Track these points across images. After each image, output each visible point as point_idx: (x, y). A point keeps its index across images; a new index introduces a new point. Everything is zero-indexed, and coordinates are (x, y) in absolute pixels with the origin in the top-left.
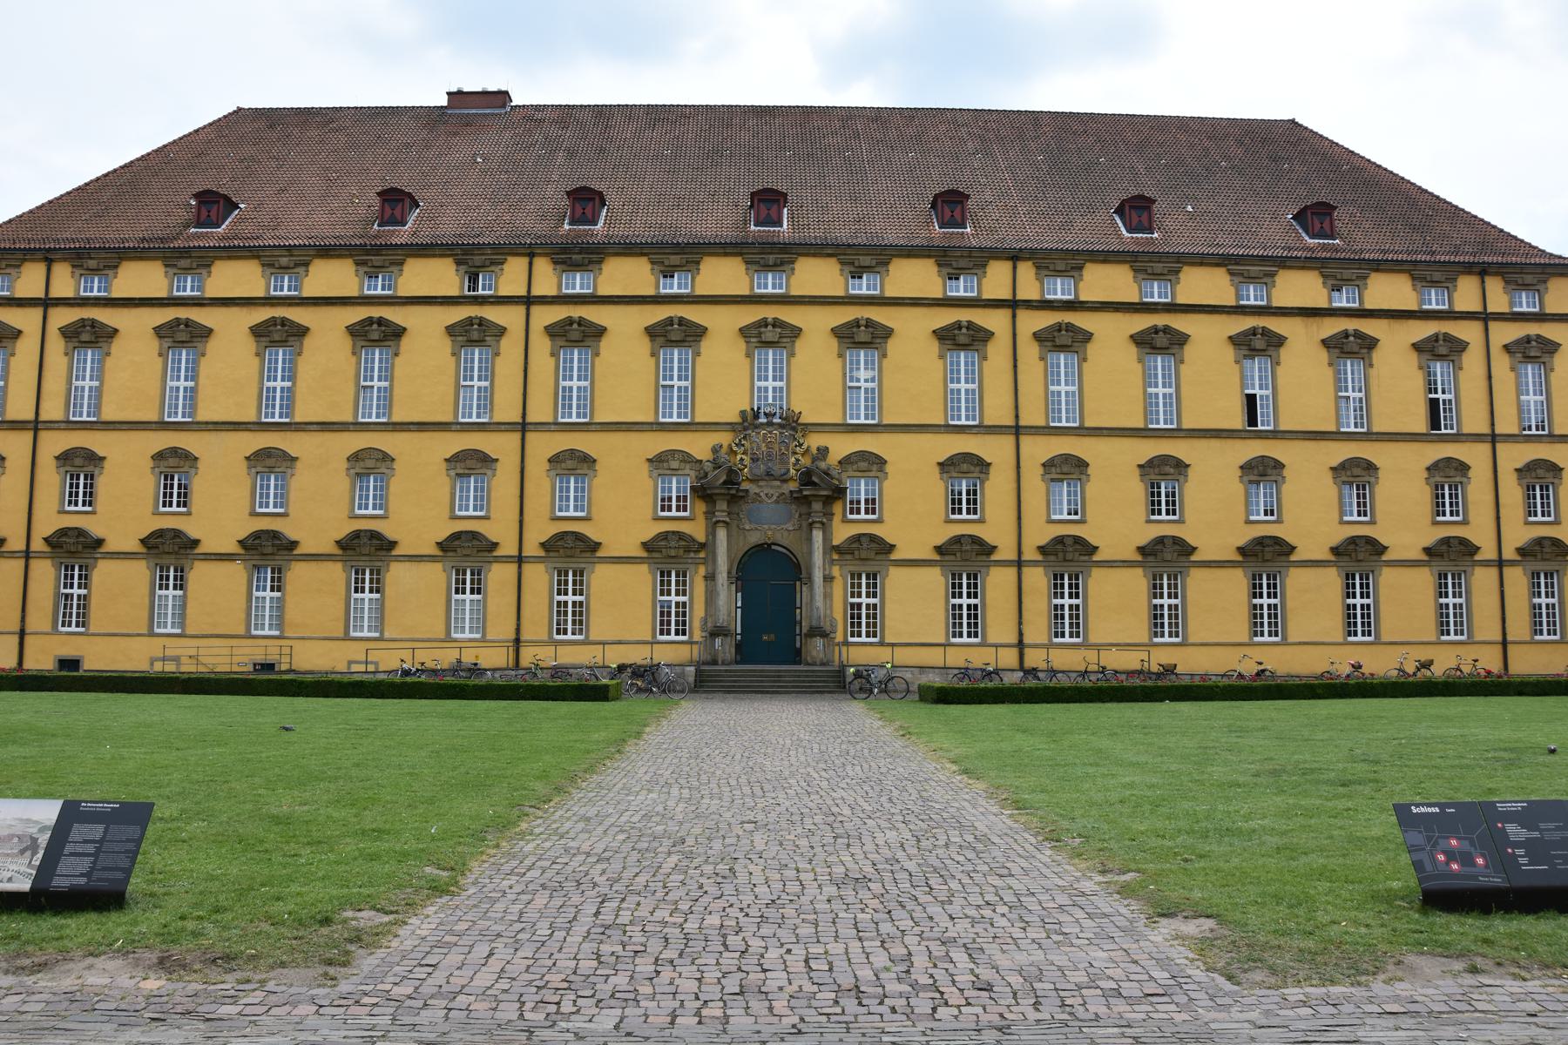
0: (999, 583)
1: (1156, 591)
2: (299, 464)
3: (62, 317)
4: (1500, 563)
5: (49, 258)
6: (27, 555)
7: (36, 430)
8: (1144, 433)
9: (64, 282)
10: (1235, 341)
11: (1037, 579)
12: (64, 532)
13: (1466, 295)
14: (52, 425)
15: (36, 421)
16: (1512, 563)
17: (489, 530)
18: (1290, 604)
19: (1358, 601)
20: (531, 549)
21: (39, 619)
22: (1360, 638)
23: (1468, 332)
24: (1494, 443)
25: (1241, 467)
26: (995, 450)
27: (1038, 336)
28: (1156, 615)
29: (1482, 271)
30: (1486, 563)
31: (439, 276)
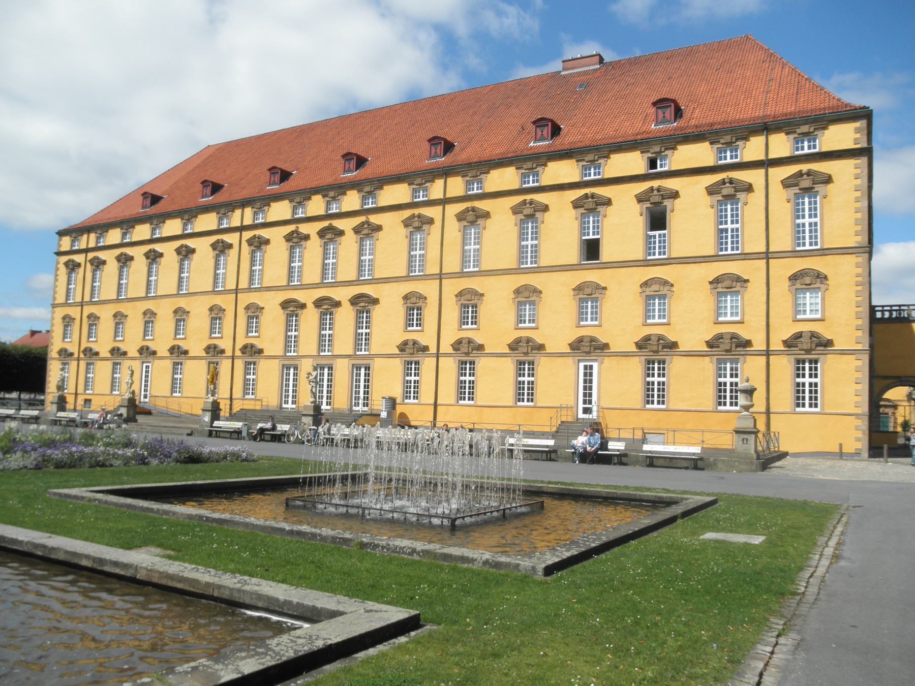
0: (428, 364)
1: (648, 373)
2: (128, 318)
4: (768, 353)
6: (78, 359)
7: (82, 306)
8: (519, 271)
11: (783, 366)
13: (753, 149)
16: (778, 353)
18: (672, 381)
19: (656, 379)
22: (655, 406)
23: (754, 177)
24: (768, 259)
25: (574, 290)
26: (429, 289)
28: (519, 386)
30: (758, 354)
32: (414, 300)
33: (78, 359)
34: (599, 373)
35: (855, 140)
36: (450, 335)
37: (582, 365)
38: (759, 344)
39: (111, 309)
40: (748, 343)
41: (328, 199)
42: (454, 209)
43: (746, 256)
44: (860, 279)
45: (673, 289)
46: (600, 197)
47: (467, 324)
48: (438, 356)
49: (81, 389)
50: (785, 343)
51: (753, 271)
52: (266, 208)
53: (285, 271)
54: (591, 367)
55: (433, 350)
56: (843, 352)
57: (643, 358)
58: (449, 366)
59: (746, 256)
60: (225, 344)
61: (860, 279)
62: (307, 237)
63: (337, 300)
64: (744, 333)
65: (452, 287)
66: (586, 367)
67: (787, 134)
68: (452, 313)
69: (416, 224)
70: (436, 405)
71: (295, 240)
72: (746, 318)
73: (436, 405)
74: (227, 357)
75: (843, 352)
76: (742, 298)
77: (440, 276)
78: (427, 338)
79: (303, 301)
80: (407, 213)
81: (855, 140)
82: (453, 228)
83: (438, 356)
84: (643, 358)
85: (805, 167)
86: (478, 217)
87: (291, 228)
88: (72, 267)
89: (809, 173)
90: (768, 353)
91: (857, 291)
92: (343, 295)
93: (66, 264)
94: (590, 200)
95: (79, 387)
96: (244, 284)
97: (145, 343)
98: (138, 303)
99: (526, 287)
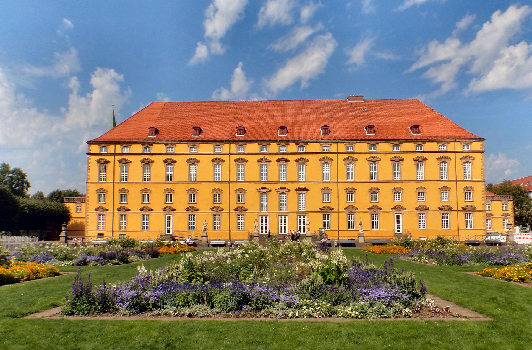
3: (118, 158)
4: (457, 211)
5: (116, 143)
7: (114, 184)
9: (119, 149)
10: (391, 160)
12: (120, 208)
13: (451, 146)
14: (118, 183)
15: (114, 182)
17: (222, 206)
20: (232, 210)
21: (116, 228)
26: (333, 187)
27: (345, 160)
29: (455, 140)
30: (454, 211)
31: (208, 148)
32: (326, 190)
33: (113, 213)
34: (402, 218)
35: (481, 148)
36: (343, 204)
37: (396, 215)
38: (455, 209)
39: (139, 187)
40: (452, 208)
41: (280, 146)
42: (342, 157)
43: (449, 181)
44: (483, 189)
45: (427, 190)
46: (400, 158)
47: (373, 200)
48: (338, 212)
49: (116, 228)
50: (462, 208)
51: (452, 185)
52: (245, 146)
53: (258, 175)
54: (399, 216)
55: (336, 210)
56: (479, 211)
57: (418, 213)
58: (343, 216)
59: (449, 181)
60: (224, 206)
61: (483, 189)
62: (270, 161)
63: (289, 189)
64: (451, 206)
65: (343, 187)
66: (397, 216)
67: (461, 143)
68: (343, 196)
69: (326, 161)
70: (338, 230)
71: (263, 162)
72: (450, 200)
73: (338, 230)
74: (110, 213)
75: (479, 211)
76: (449, 194)
77: (338, 182)
78: (333, 205)
79: (270, 188)
80: (321, 156)
81: (481, 148)
82: (342, 164)
83: (338, 212)
84: (418, 213)
85: (467, 154)
86: (353, 160)
87: (261, 157)
88: (102, 163)
89: (469, 156)
90: (457, 211)
91: (482, 193)
92: (292, 187)
93: (98, 161)
94: (397, 158)
95: (114, 228)
96: (233, 179)
97: (167, 205)
98: (160, 185)
99: (374, 188)
